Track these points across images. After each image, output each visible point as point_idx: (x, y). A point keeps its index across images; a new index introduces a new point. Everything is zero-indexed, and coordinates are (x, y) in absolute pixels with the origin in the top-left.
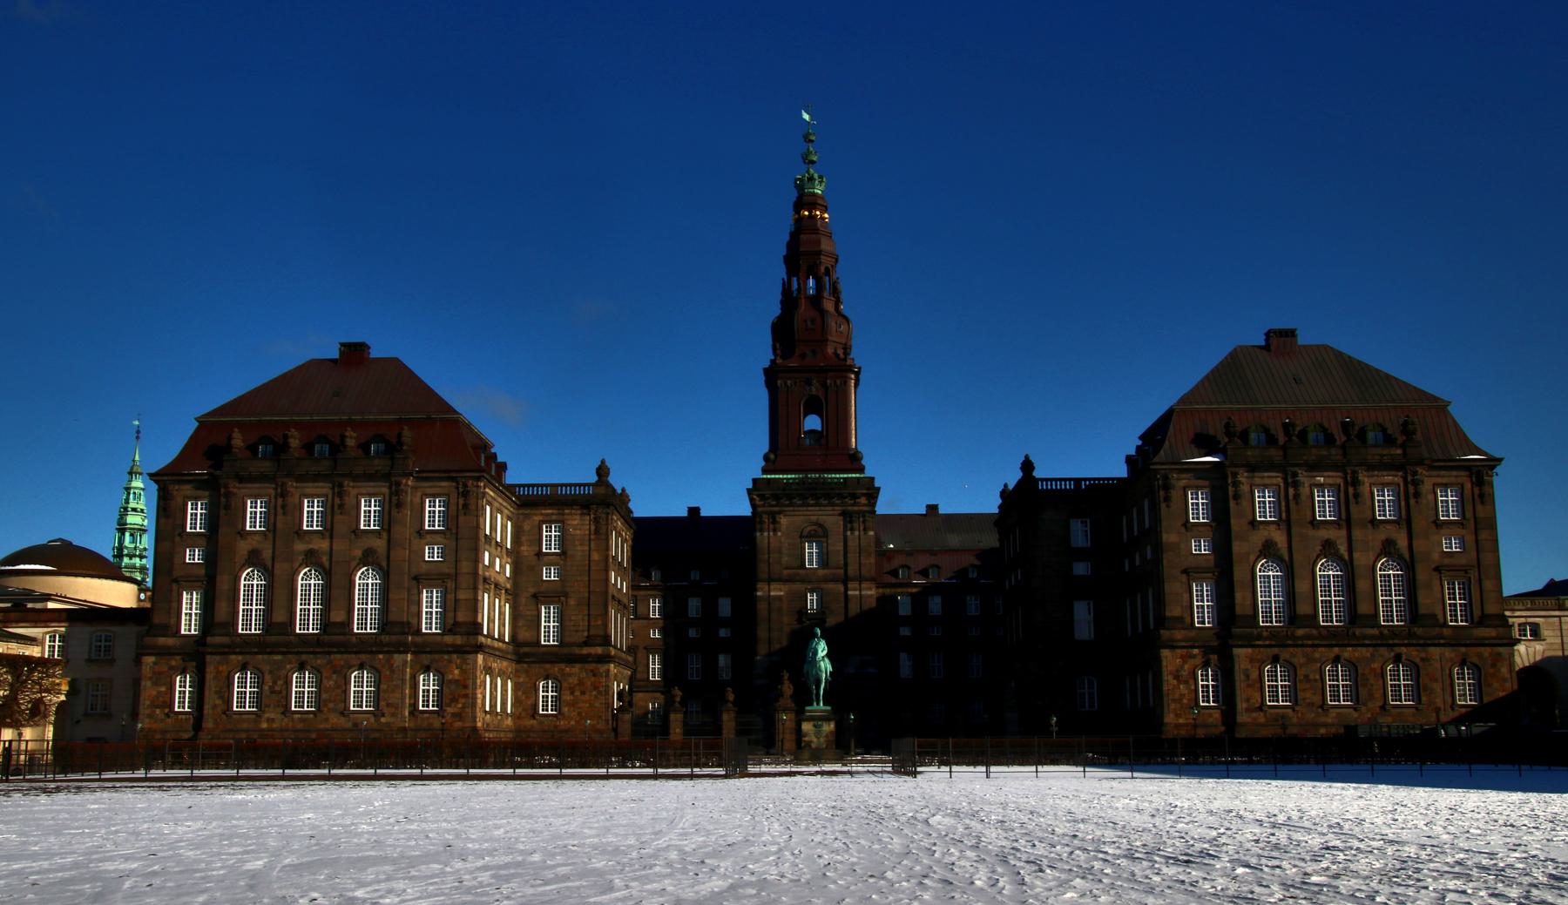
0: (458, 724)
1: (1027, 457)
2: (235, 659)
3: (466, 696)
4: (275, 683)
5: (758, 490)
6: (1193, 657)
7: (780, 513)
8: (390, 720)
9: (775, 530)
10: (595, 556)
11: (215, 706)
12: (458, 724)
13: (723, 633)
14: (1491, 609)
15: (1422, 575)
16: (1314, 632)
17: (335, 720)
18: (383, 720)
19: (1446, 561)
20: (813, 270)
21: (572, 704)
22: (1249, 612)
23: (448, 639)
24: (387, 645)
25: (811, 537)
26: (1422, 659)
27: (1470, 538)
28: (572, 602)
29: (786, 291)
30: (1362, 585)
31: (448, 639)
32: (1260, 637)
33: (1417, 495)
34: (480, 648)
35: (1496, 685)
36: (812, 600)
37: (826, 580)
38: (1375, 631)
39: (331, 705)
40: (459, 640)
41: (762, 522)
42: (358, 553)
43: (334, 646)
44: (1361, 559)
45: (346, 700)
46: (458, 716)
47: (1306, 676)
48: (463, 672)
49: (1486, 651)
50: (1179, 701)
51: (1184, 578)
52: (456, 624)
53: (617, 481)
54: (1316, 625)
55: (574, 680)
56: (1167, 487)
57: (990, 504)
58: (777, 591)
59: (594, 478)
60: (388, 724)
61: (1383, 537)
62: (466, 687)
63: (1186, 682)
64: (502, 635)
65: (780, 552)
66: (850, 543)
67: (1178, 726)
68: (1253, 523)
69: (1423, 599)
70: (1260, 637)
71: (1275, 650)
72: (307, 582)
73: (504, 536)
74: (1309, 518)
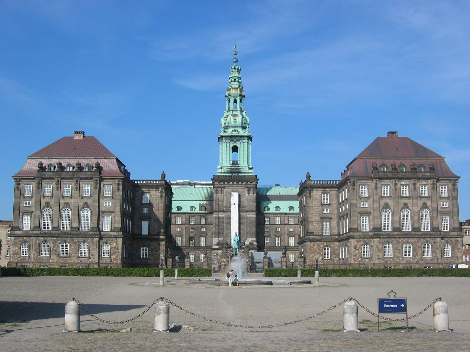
0: (115, 262)
1: (308, 173)
3: (118, 252)
4: (54, 247)
6: (360, 241)
7: (224, 188)
8: (93, 260)
9: (222, 193)
10: (160, 205)
11: (34, 254)
12: (115, 262)
13: (203, 230)
16: (400, 233)
17: (75, 260)
18: (90, 260)
19: (442, 210)
21: (153, 255)
22: (379, 226)
23: (112, 233)
24: (91, 235)
26: (434, 242)
27: (450, 203)
28: (152, 220)
30: (416, 218)
31: (112, 233)
32: (382, 235)
33: (434, 188)
35: (456, 250)
38: (419, 233)
39: (73, 255)
40: (115, 234)
41: (217, 191)
42: (82, 204)
46: (115, 259)
47: (397, 248)
48: (117, 244)
49: (454, 240)
50: (355, 256)
51: (359, 215)
52: (115, 228)
54: (401, 231)
55: (153, 247)
56: (354, 185)
59: (160, 178)
60: (92, 261)
61: (422, 202)
62: (118, 249)
63: (358, 250)
64: (129, 231)
65: (223, 201)
66: (248, 198)
67: (355, 264)
68: (382, 197)
70: (382, 235)
71: (387, 239)
73: (129, 198)
74: (399, 195)
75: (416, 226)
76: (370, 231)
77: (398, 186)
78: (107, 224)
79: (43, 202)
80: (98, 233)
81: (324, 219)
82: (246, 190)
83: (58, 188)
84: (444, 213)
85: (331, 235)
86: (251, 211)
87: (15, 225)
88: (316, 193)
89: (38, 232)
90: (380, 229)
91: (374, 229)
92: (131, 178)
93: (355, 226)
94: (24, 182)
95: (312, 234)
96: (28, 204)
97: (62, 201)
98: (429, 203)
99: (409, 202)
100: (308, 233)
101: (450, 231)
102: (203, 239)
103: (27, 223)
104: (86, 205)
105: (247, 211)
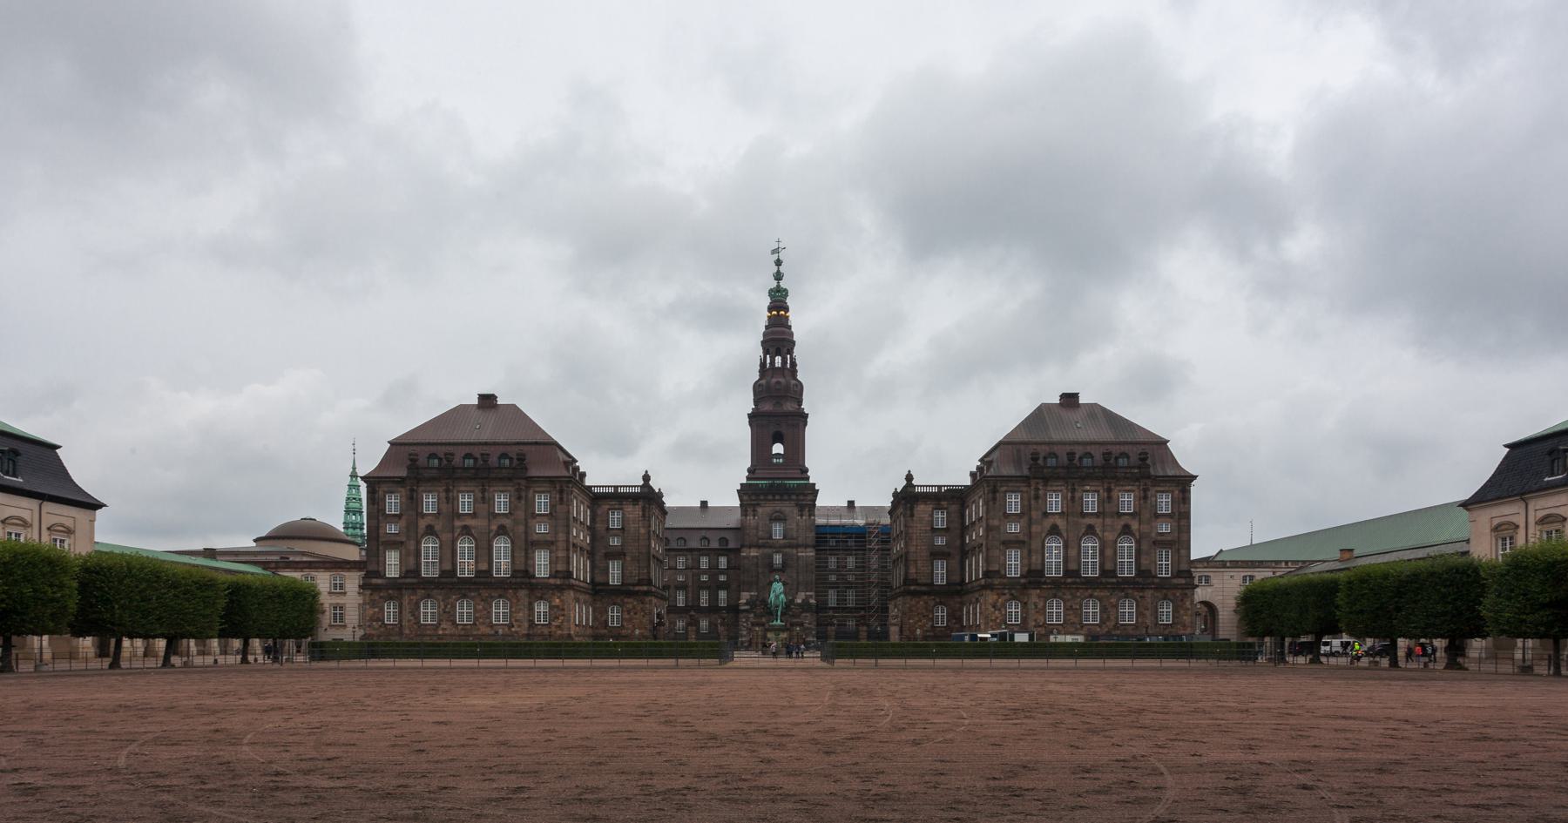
2: (421, 592)
5: (743, 491)
13: (722, 578)
14: (1184, 567)
15: (1144, 547)
20: (778, 353)
25: (777, 519)
29: (763, 364)
30: (1109, 552)
31: (552, 581)
34: (571, 587)
36: (778, 559)
37: (785, 546)
42: (494, 527)
43: (483, 584)
44: (1109, 536)
45: (490, 617)
53: (655, 484)
56: (995, 491)
57: (887, 502)
58: (754, 553)
65: (757, 528)
68: (1046, 514)
69: (1144, 561)
72: (465, 546)
75: (1108, 566)
76: (1022, 576)
77: (1077, 495)
78: (542, 564)
79: (422, 524)
80: (522, 579)
81: (936, 554)
82: (796, 511)
83: (447, 498)
84: (1161, 543)
85: (948, 583)
86: (806, 546)
87: (372, 567)
88: (922, 509)
89: (411, 582)
90: (1041, 572)
91: (1029, 571)
92: (588, 482)
93: (995, 567)
94: (384, 487)
95: (915, 582)
96: (392, 529)
97: (458, 523)
98: (1135, 526)
99: (1097, 522)
100: (907, 581)
101: (1173, 577)
102: (723, 595)
103: (392, 564)
104: (502, 531)
105: (797, 546)
